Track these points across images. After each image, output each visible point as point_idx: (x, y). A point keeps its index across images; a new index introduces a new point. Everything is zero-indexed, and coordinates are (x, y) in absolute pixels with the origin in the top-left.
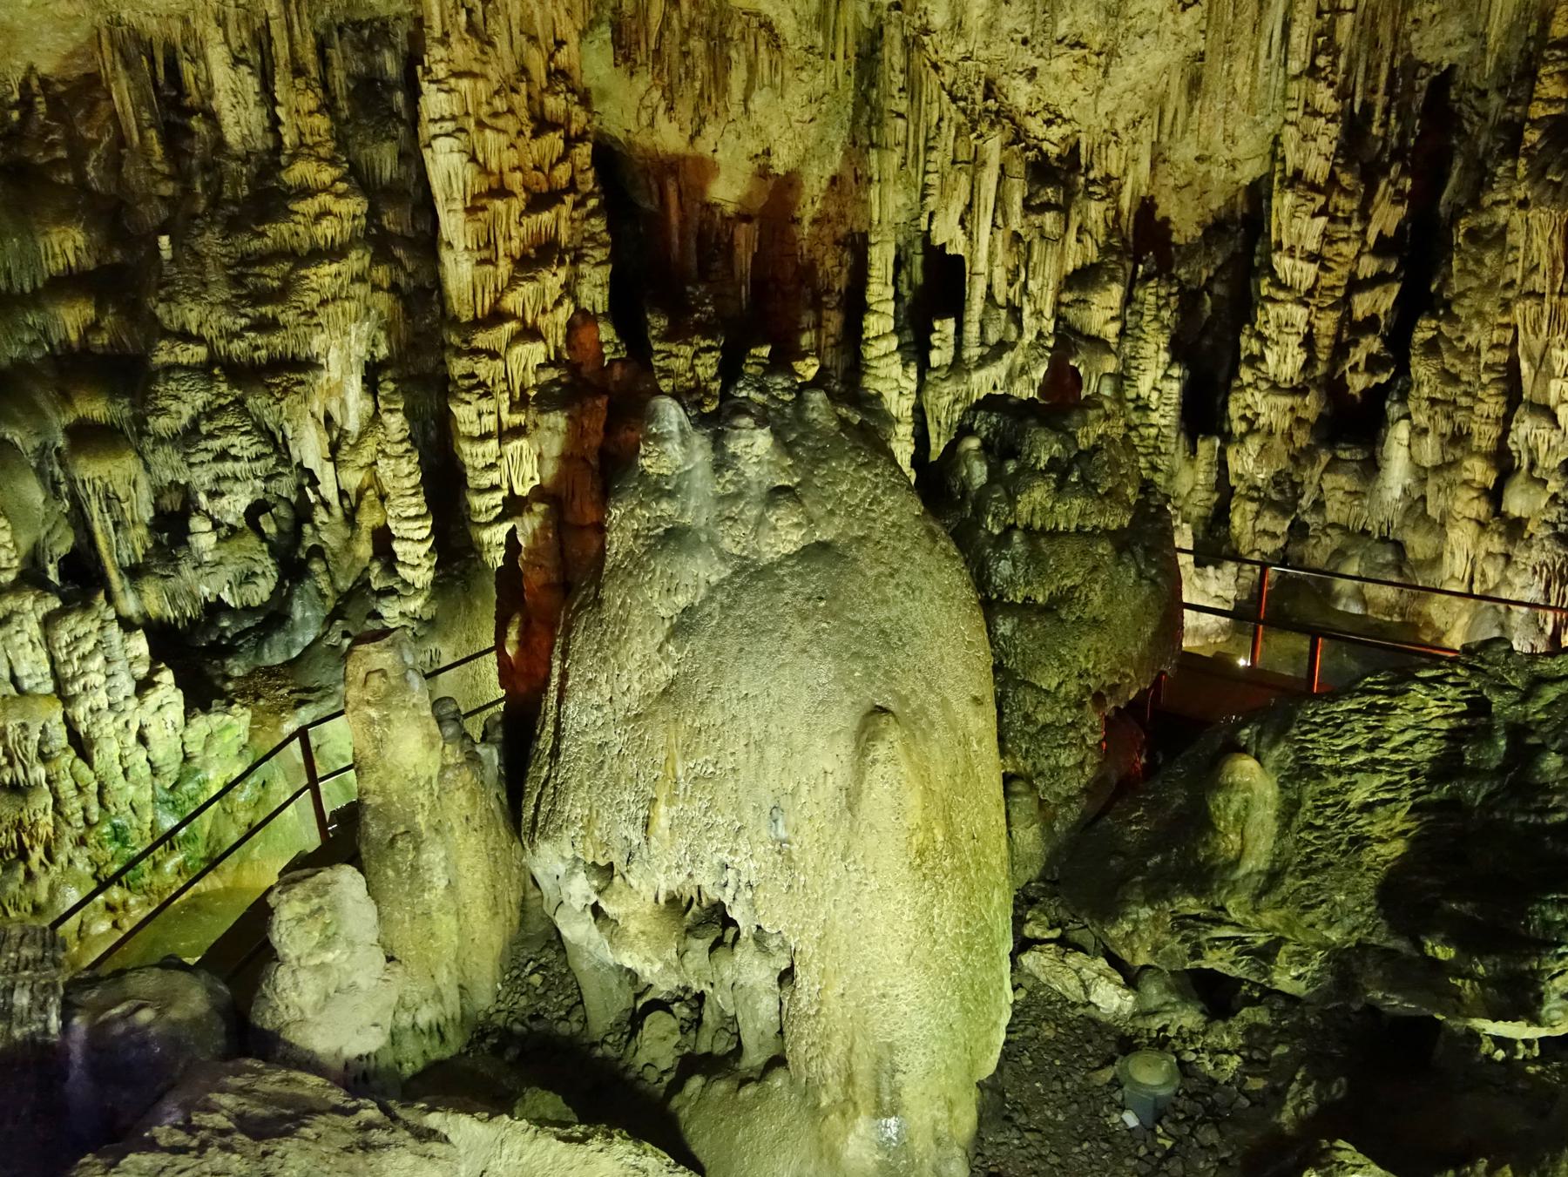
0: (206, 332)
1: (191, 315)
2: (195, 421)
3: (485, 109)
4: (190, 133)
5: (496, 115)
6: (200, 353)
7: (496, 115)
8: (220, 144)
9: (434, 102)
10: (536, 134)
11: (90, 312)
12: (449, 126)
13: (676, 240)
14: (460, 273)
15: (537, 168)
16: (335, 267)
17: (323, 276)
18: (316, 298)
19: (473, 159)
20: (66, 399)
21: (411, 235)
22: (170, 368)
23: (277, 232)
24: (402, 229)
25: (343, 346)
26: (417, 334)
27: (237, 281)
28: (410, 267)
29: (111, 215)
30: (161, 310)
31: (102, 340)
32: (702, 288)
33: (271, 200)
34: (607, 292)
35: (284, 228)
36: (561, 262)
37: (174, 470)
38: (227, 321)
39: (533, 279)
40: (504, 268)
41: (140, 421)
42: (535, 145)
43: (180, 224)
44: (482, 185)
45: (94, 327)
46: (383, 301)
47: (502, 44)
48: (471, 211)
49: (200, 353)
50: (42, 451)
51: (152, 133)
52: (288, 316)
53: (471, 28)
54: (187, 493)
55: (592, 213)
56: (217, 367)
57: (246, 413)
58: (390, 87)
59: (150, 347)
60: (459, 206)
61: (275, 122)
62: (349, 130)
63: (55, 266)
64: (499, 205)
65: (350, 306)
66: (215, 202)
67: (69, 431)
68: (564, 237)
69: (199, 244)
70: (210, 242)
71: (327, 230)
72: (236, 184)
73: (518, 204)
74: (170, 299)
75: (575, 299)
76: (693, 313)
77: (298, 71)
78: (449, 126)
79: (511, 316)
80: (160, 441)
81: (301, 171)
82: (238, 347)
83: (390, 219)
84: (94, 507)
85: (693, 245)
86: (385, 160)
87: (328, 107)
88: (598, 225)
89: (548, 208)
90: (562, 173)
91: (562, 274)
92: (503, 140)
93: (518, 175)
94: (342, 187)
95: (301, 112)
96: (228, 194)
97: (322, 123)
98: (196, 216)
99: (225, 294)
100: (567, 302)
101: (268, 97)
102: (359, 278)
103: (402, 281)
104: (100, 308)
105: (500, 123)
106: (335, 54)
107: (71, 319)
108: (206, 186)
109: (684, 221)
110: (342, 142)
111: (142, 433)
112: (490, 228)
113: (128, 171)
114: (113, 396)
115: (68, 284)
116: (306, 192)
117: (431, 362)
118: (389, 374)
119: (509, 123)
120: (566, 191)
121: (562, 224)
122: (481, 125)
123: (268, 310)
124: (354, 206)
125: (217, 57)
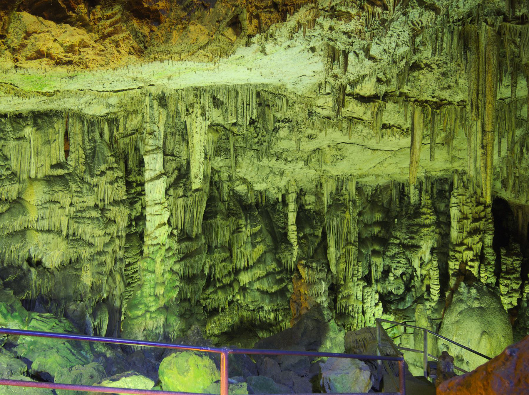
0: (400, 238)
1: (398, 234)
2: (395, 254)
3: (465, 202)
4: (404, 200)
5: (467, 203)
6: (398, 241)
7: (467, 203)
8: (409, 202)
9: (453, 200)
10: (477, 206)
11: (380, 229)
12: (456, 205)
13: (521, 226)
14: (454, 234)
15: (476, 213)
16: (427, 229)
17: (425, 230)
18: (423, 234)
19: (460, 211)
20: (372, 245)
21: (446, 222)
22: (392, 243)
23: (417, 221)
24: (443, 223)
25: (427, 245)
26: (444, 243)
27: (408, 229)
28: (444, 229)
29: (387, 211)
30: (393, 232)
31: (380, 235)
32: (517, 245)
33: (417, 214)
34: (492, 241)
35: (419, 220)
36: (480, 234)
37: (389, 263)
38: (404, 236)
39: (472, 237)
40: (465, 234)
41: (384, 252)
42: (476, 208)
43: (399, 216)
44: (462, 216)
45: (380, 232)
46: (437, 236)
47: (471, 189)
48: (459, 222)
49: (398, 241)
50: (367, 254)
51: (397, 200)
52: (417, 237)
53: (464, 186)
54: (389, 267)
55: (490, 223)
56: (401, 244)
57: (405, 255)
58: (445, 192)
59: (389, 239)
60: (456, 220)
61: (420, 200)
62: (436, 200)
63: (375, 220)
64: (465, 221)
65: (430, 237)
66: (406, 213)
67: (372, 251)
68: (481, 228)
69: (402, 221)
70: (404, 221)
71: (427, 221)
72: (411, 210)
73: (470, 221)
74: (395, 231)
75: (483, 242)
76: (513, 250)
77: (427, 192)
78: (456, 205)
79: (465, 245)
80: (388, 257)
81: (424, 210)
82: (406, 241)
83: (441, 219)
84: (373, 266)
85: (526, 227)
86: (442, 207)
87: (431, 198)
88: (491, 226)
89: (477, 222)
90: (483, 214)
91: (480, 236)
92: (468, 208)
93: (471, 215)
94: (431, 214)
95: (426, 199)
96: (409, 212)
97: (430, 201)
98: (402, 216)
99: (405, 231)
100: (480, 243)
101: (420, 195)
102: (432, 231)
103: (442, 232)
104: (382, 229)
105: (468, 204)
106: (435, 186)
107: (376, 230)
108: (405, 210)
109: (524, 221)
110: (433, 204)
111: (384, 254)
112: (463, 225)
113: (392, 205)
114: (381, 246)
115: (377, 223)
116: (424, 214)
117: (446, 250)
118: (436, 251)
119: (470, 204)
120: (483, 218)
121: (481, 225)
122: (463, 205)
123: (413, 235)
124: (433, 218)
125: (412, 188)
